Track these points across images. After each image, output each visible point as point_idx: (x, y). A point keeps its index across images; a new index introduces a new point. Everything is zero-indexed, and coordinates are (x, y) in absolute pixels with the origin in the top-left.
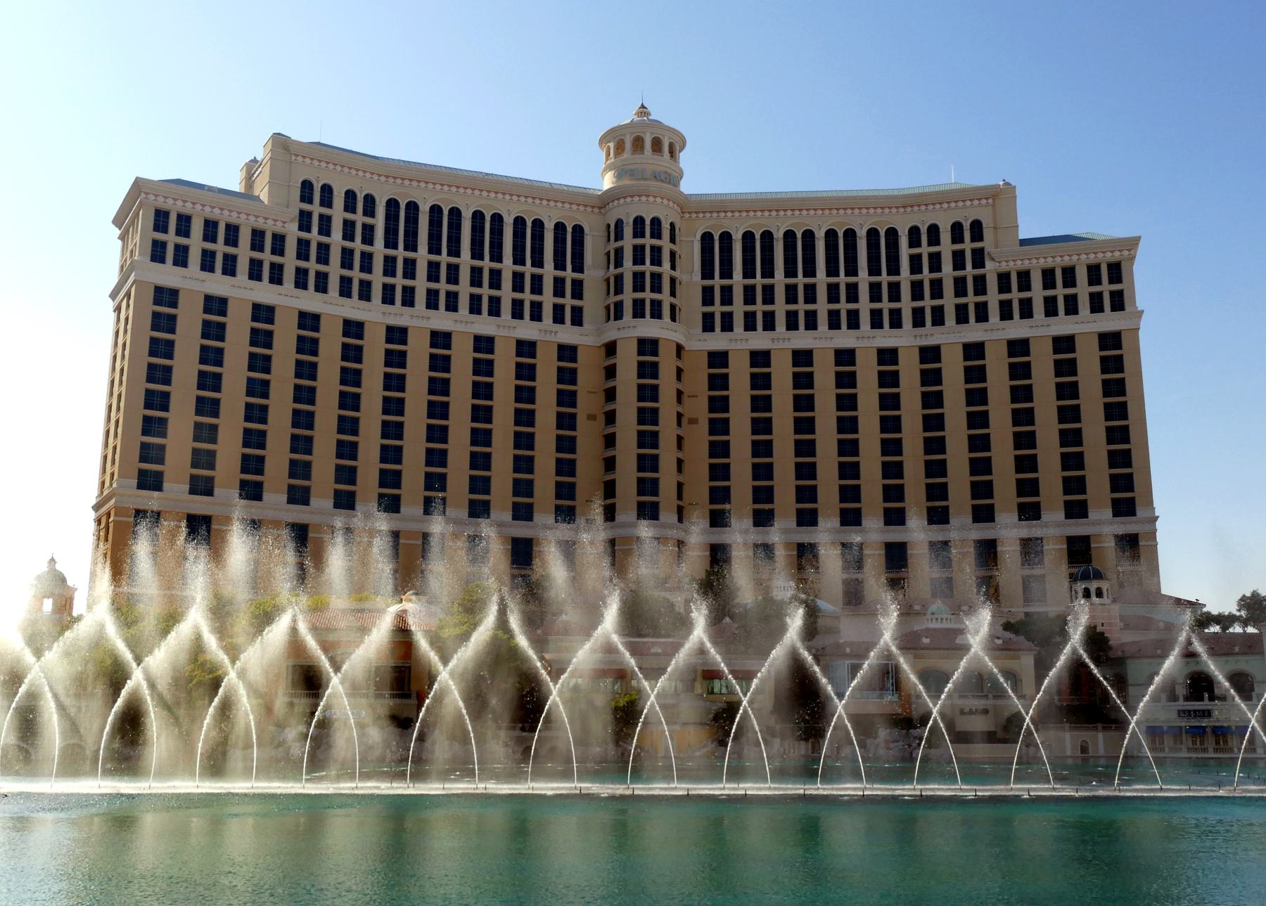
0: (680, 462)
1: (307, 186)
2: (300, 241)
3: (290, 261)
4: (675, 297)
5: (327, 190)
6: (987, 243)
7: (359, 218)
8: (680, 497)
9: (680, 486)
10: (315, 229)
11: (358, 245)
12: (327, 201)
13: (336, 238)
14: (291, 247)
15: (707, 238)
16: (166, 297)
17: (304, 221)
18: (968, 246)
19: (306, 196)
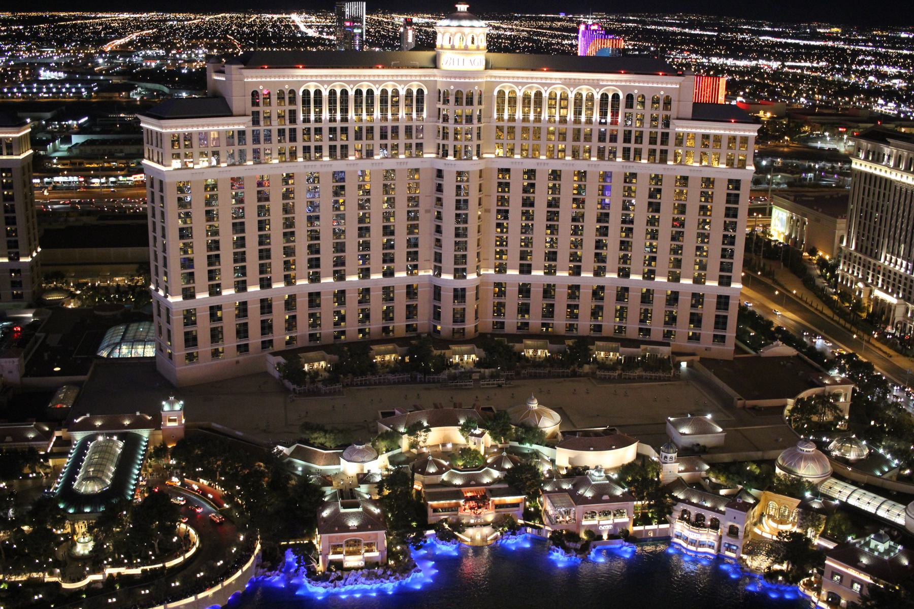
1: (255, 94)
6: (673, 113)
14: (249, 137)
19: (255, 103)
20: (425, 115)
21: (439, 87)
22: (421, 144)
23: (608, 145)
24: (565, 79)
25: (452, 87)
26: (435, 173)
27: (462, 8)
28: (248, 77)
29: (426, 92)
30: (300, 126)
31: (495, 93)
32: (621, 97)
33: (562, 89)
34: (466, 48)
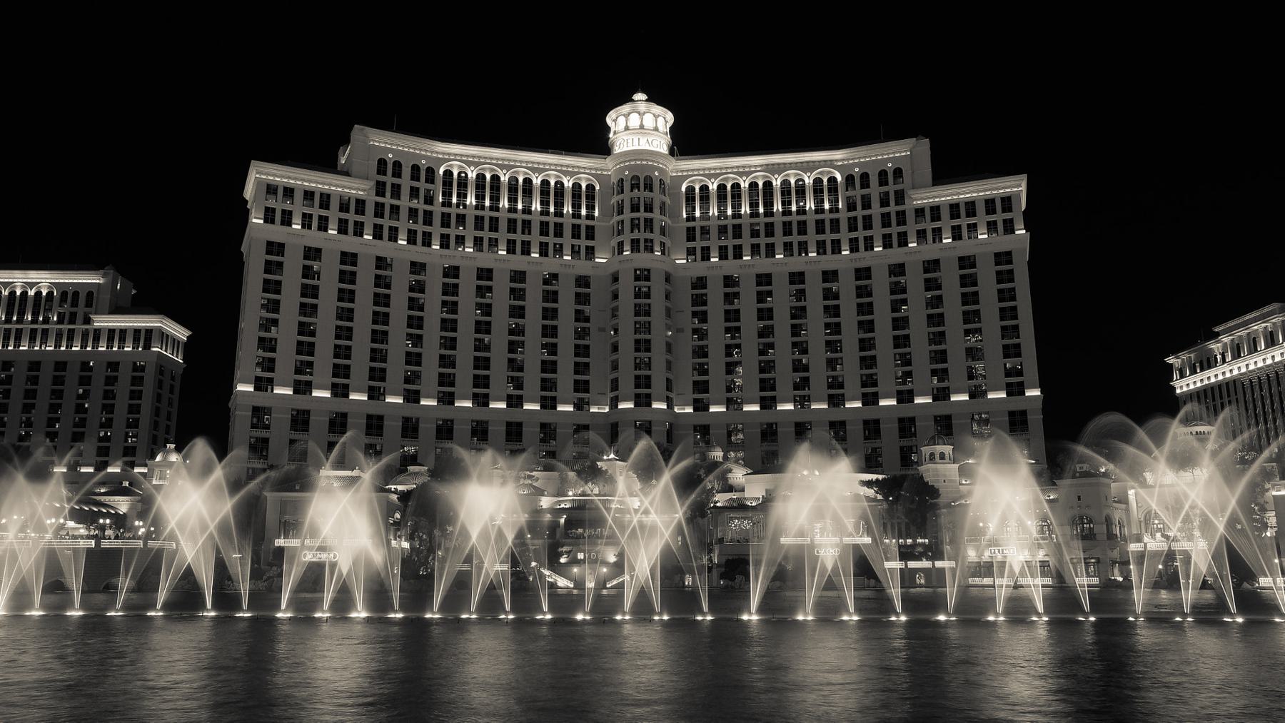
0: (669, 363)
1: (382, 163)
2: (377, 204)
3: (369, 219)
4: (664, 235)
5: (397, 165)
7: (422, 185)
8: (669, 388)
9: (667, 379)
10: (388, 194)
11: (420, 205)
12: (397, 172)
13: (405, 202)
14: (370, 209)
15: (691, 190)
16: (275, 249)
17: (380, 190)
18: (891, 188)
20: (596, 214)
21: (613, 180)
22: (593, 248)
23: (828, 237)
24: (767, 165)
25: (627, 173)
26: (610, 280)
27: (640, 96)
28: (373, 141)
29: (597, 188)
30: (437, 209)
31: (683, 189)
32: (839, 177)
33: (764, 177)
34: (642, 127)
